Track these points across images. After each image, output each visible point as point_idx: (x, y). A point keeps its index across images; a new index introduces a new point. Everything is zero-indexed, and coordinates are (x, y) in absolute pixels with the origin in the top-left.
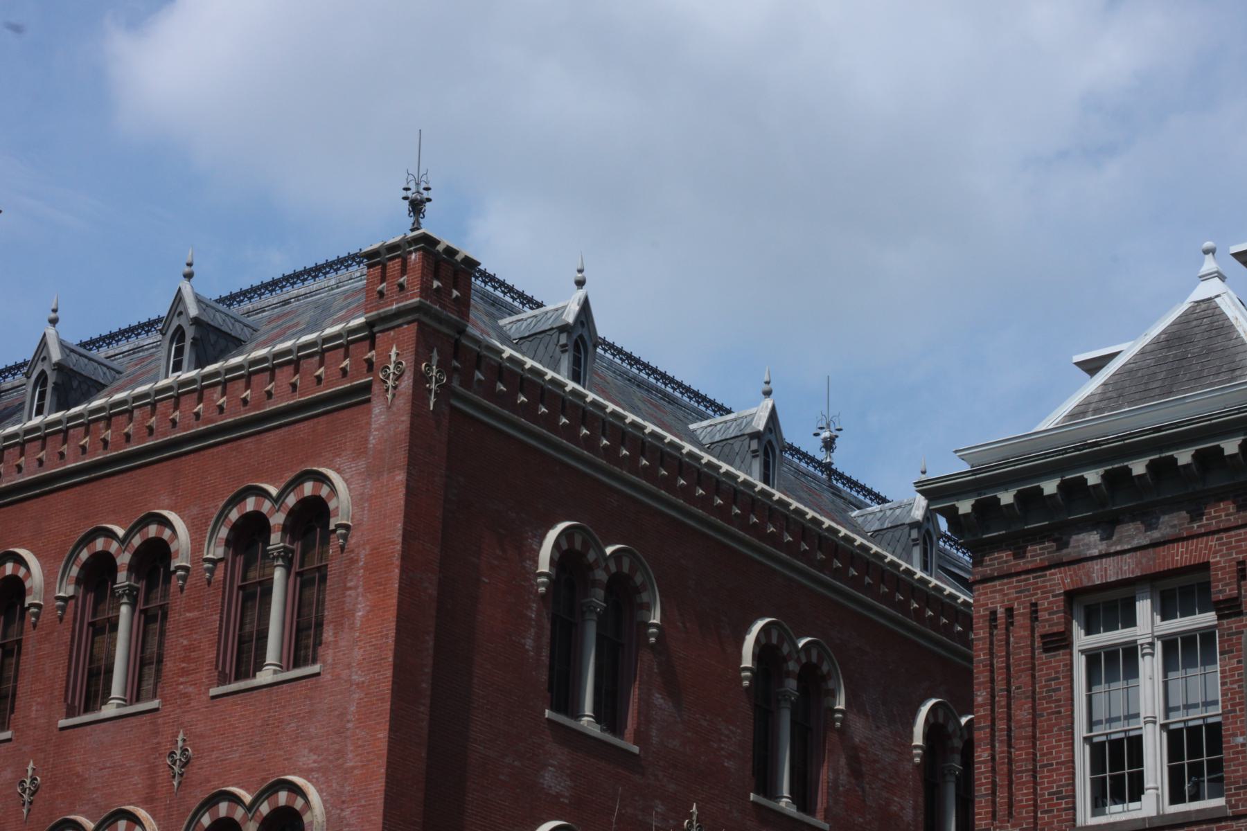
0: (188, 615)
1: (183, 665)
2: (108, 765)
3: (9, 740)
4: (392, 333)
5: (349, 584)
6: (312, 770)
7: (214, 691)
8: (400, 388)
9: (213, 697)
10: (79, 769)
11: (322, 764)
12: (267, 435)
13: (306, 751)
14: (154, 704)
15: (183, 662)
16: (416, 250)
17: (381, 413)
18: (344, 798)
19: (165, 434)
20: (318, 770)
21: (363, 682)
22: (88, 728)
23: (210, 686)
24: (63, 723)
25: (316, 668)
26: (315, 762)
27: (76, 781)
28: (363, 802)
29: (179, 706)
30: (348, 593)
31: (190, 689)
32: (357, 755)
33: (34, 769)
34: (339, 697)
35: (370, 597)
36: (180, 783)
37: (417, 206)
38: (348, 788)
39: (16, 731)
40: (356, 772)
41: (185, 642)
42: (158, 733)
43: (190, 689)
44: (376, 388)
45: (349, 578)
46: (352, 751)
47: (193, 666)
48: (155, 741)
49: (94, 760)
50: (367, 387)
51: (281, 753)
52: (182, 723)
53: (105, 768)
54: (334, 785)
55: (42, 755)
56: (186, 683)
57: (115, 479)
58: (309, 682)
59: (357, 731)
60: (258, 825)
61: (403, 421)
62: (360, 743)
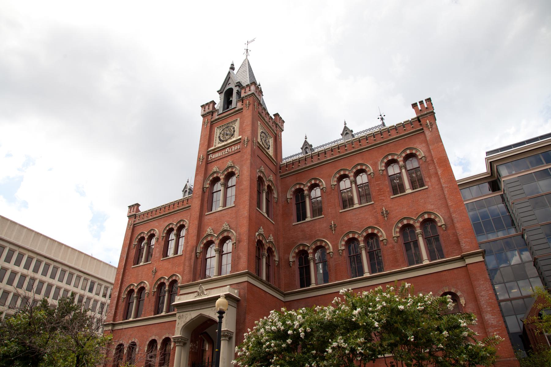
0: (376, 183)
1: (379, 193)
2: (360, 218)
3: (323, 217)
4: (425, 118)
5: (430, 169)
6: (434, 209)
7: (392, 197)
8: (433, 127)
9: (392, 198)
10: (350, 220)
11: (437, 207)
12: (390, 144)
13: (430, 205)
14: (373, 202)
15: (379, 192)
16: (428, 101)
17: (428, 133)
18: (451, 212)
19: (358, 148)
20: (436, 209)
21: (447, 186)
22: (350, 211)
23: (391, 196)
24: (341, 211)
25: (427, 187)
26: (434, 207)
27: (349, 223)
28: (459, 212)
29: (381, 202)
30: (430, 170)
31: (383, 198)
32: (452, 202)
33: (334, 223)
34: (437, 192)
35: (442, 168)
36: (387, 219)
37: (382, 119)
38: (452, 210)
39: (324, 215)
40: (453, 206)
41: (378, 188)
42: (375, 209)
43: (383, 198)
44: (424, 129)
45: (429, 167)
46: (450, 202)
47: (382, 193)
48: (375, 211)
49: (354, 218)
50: (422, 129)
51: (421, 207)
52: (383, 205)
53: (359, 219)
54: (443, 211)
55: (336, 219)
56: (381, 197)
57: (342, 160)
58: (425, 191)
59: (450, 197)
60: (420, 224)
61: (437, 133)
62: (452, 199)
